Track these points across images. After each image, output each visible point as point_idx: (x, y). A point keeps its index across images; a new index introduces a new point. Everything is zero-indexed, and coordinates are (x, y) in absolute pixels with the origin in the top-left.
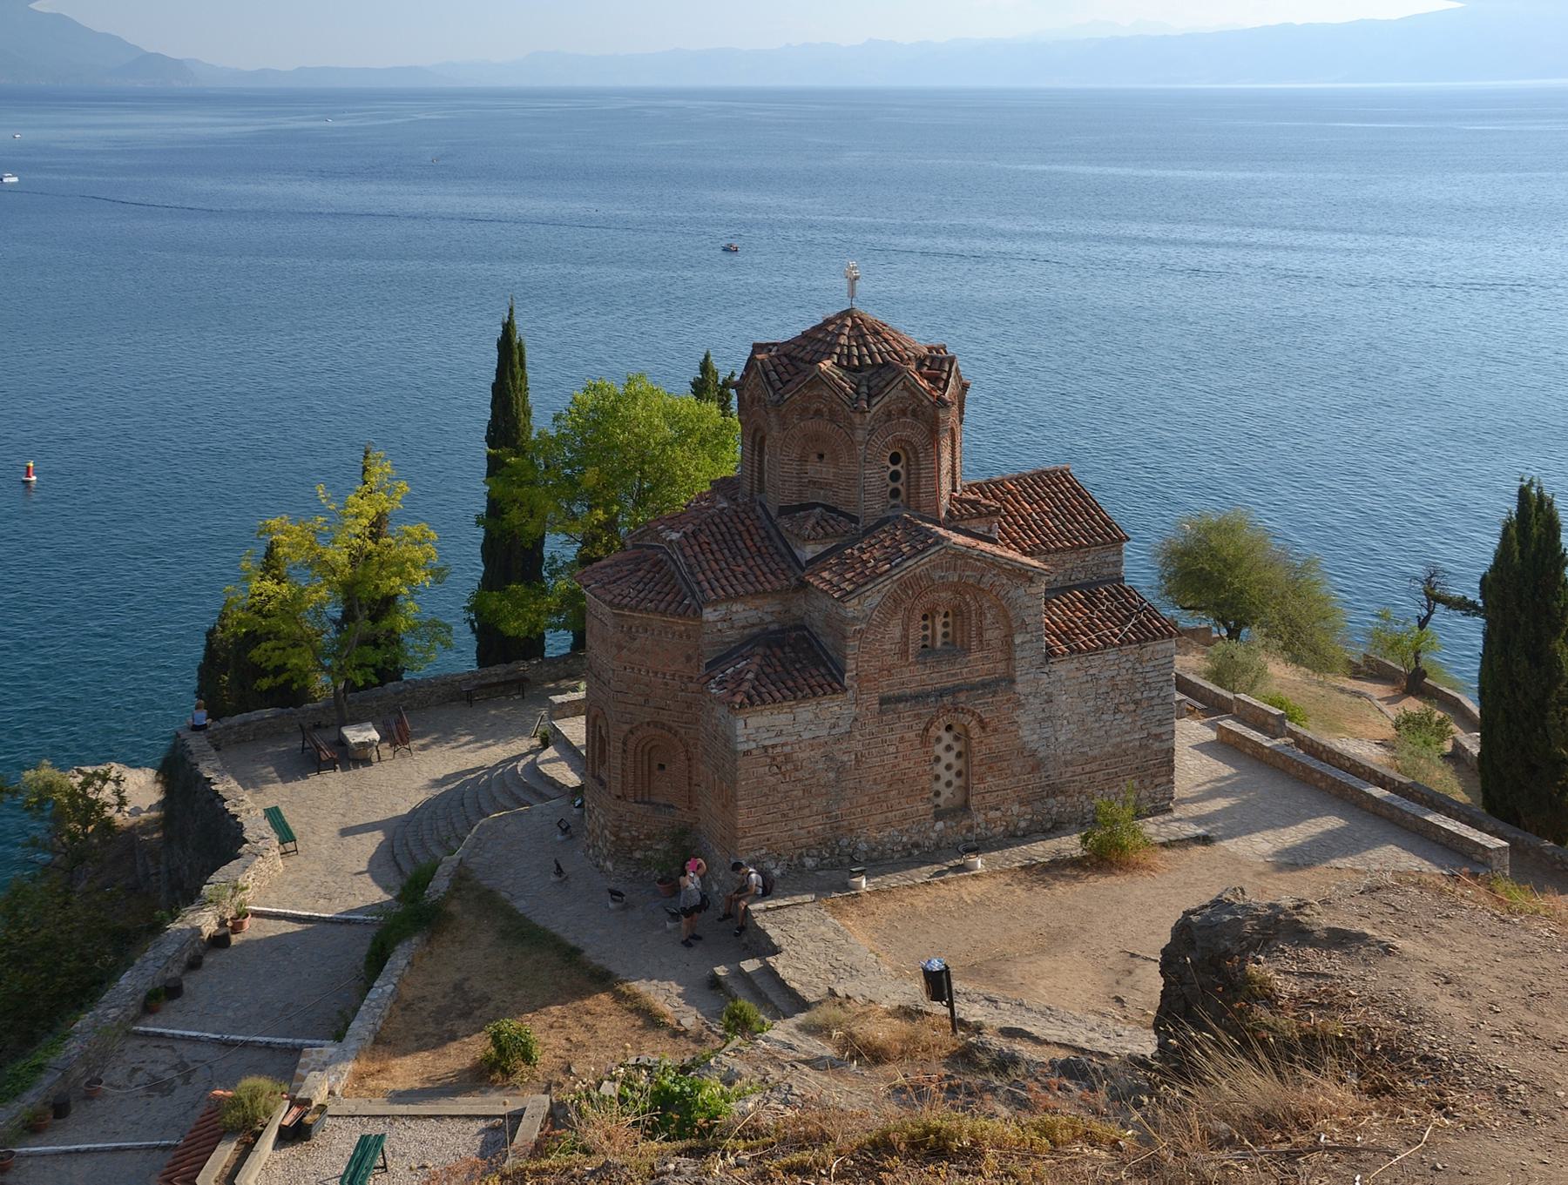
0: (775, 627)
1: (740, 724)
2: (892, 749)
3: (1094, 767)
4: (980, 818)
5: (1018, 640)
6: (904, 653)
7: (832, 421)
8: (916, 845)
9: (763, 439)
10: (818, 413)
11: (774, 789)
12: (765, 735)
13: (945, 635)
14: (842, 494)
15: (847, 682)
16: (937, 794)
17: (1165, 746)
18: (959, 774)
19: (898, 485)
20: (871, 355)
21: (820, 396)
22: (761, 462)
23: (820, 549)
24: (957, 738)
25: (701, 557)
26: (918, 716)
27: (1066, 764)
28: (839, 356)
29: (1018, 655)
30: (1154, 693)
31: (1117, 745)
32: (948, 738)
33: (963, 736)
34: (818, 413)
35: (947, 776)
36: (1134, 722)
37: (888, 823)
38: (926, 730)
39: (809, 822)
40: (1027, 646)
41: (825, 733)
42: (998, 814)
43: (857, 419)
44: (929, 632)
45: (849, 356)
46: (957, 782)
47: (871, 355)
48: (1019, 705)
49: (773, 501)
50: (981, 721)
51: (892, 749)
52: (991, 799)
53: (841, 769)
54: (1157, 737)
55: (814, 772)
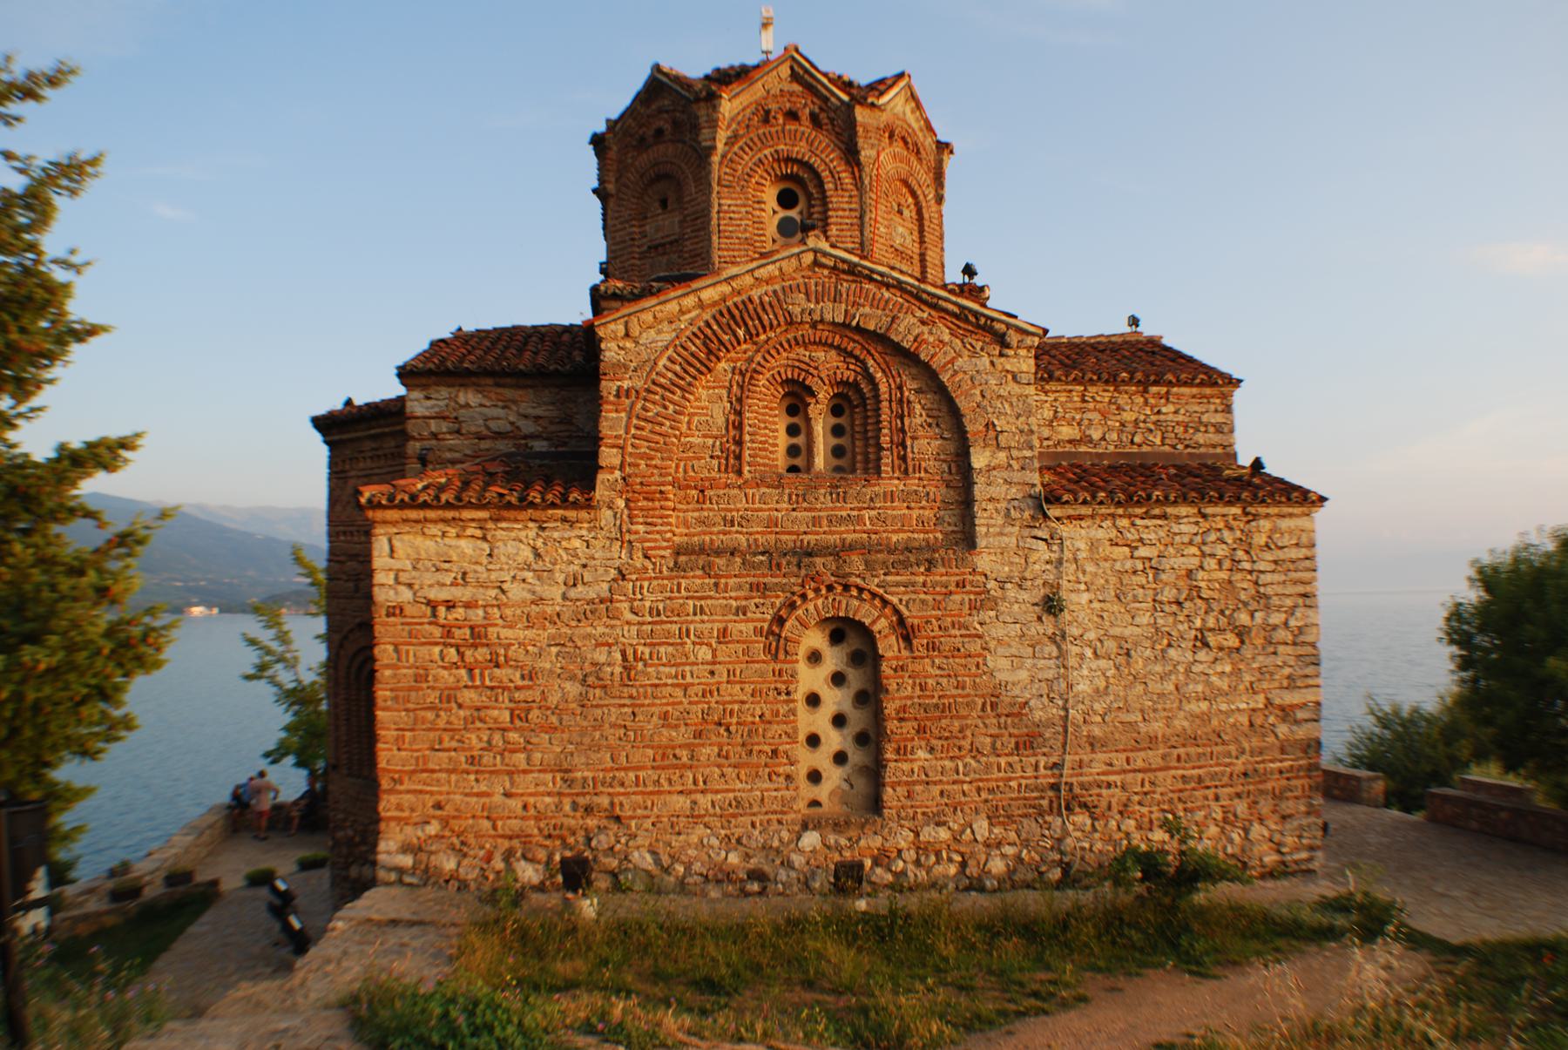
0: (539, 446)
1: (380, 546)
2: (704, 653)
3: (1154, 757)
4: (904, 839)
5: (979, 460)
6: (733, 458)
8: (757, 875)
10: (659, 132)
11: (449, 697)
12: (429, 578)
13: (837, 452)
15: (601, 493)
16: (815, 777)
17: (1301, 732)
18: (862, 739)
24: (856, 659)
26: (761, 589)
27: (1093, 743)
29: (979, 491)
30: (1277, 618)
31: (1205, 718)
32: (833, 659)
33: (865, 655)
35: (834, 740)
36: (1237, 672)
37: (694, 817)
38: (780, 621)
39: (525, 783)
40: (999, 475)
41: (556, 592)
42: (944, 834)
44: (800, 440)
46: (856, 756)
48: (993, 603)
50: (901, 621)
51: (704, 653)
52: (929, 798)
53: (591, 678)
54: (1286, 713)
55: (531, 676)
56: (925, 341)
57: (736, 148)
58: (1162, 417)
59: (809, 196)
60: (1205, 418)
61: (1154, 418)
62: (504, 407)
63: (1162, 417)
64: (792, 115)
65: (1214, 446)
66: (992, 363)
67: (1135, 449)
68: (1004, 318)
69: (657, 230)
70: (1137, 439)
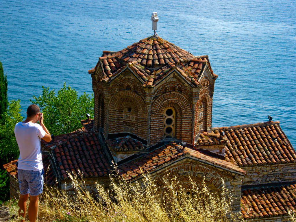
7: (136, 92)
9: (103, 100)
10: (128, 88)
14: (140, 129)
19: (167, 126)
20: (159, 60)
21: (129, 79)
22: (103, 112)
23: (126, 156)
25: (64, 157)
28: (143, 59)
34: (128, 88)
43: (147, 92)
45: (148, 60)
47: (159, 60)
49: (107, 132)
56: (214, 179)
57: (156, 101)
58: (276, 173)
59: (176, 113)
60: (289, 171)
61: (273, 173)
62: (89, 186)
63: (276, 173)
64: (174, 89)
65: (290, 180)
66: (231, 183)
67: (267, 183)
68: (235, 172)
69: (127, 117)
70: (268, 180)
